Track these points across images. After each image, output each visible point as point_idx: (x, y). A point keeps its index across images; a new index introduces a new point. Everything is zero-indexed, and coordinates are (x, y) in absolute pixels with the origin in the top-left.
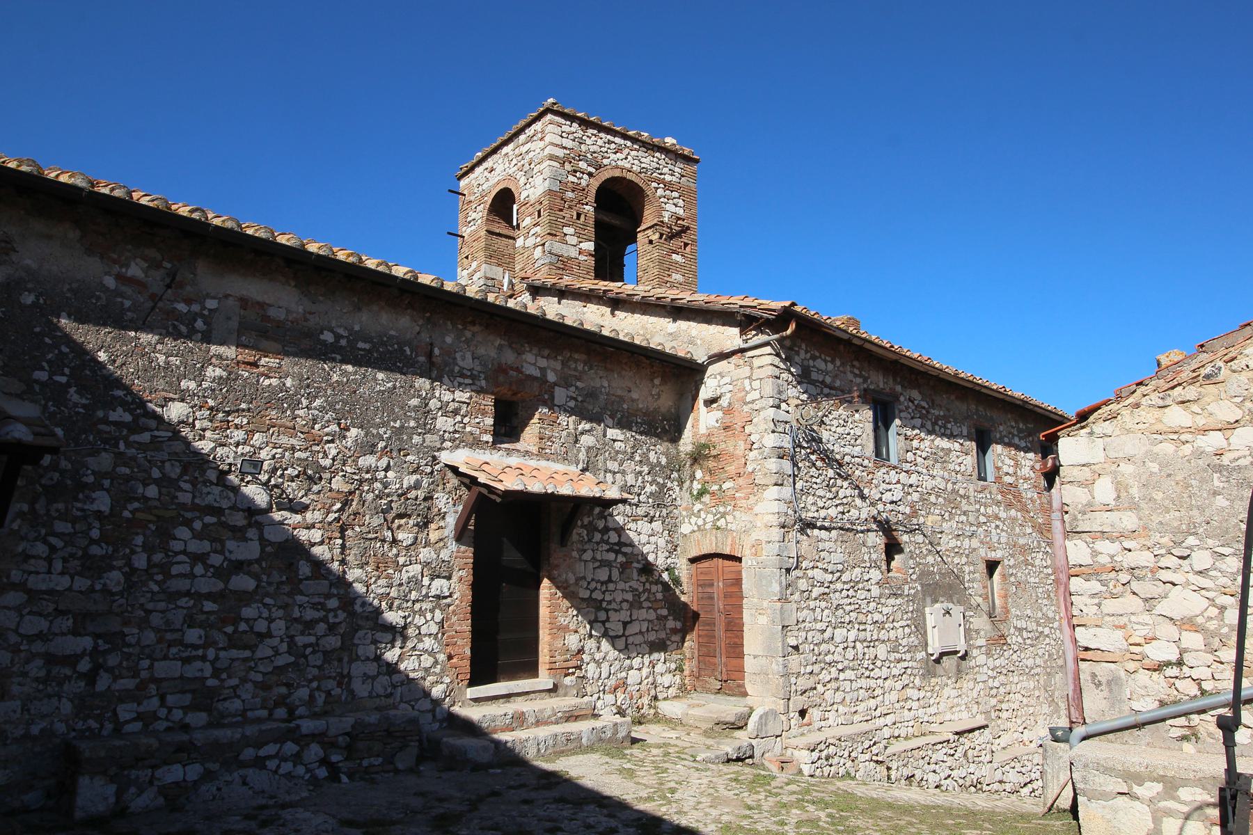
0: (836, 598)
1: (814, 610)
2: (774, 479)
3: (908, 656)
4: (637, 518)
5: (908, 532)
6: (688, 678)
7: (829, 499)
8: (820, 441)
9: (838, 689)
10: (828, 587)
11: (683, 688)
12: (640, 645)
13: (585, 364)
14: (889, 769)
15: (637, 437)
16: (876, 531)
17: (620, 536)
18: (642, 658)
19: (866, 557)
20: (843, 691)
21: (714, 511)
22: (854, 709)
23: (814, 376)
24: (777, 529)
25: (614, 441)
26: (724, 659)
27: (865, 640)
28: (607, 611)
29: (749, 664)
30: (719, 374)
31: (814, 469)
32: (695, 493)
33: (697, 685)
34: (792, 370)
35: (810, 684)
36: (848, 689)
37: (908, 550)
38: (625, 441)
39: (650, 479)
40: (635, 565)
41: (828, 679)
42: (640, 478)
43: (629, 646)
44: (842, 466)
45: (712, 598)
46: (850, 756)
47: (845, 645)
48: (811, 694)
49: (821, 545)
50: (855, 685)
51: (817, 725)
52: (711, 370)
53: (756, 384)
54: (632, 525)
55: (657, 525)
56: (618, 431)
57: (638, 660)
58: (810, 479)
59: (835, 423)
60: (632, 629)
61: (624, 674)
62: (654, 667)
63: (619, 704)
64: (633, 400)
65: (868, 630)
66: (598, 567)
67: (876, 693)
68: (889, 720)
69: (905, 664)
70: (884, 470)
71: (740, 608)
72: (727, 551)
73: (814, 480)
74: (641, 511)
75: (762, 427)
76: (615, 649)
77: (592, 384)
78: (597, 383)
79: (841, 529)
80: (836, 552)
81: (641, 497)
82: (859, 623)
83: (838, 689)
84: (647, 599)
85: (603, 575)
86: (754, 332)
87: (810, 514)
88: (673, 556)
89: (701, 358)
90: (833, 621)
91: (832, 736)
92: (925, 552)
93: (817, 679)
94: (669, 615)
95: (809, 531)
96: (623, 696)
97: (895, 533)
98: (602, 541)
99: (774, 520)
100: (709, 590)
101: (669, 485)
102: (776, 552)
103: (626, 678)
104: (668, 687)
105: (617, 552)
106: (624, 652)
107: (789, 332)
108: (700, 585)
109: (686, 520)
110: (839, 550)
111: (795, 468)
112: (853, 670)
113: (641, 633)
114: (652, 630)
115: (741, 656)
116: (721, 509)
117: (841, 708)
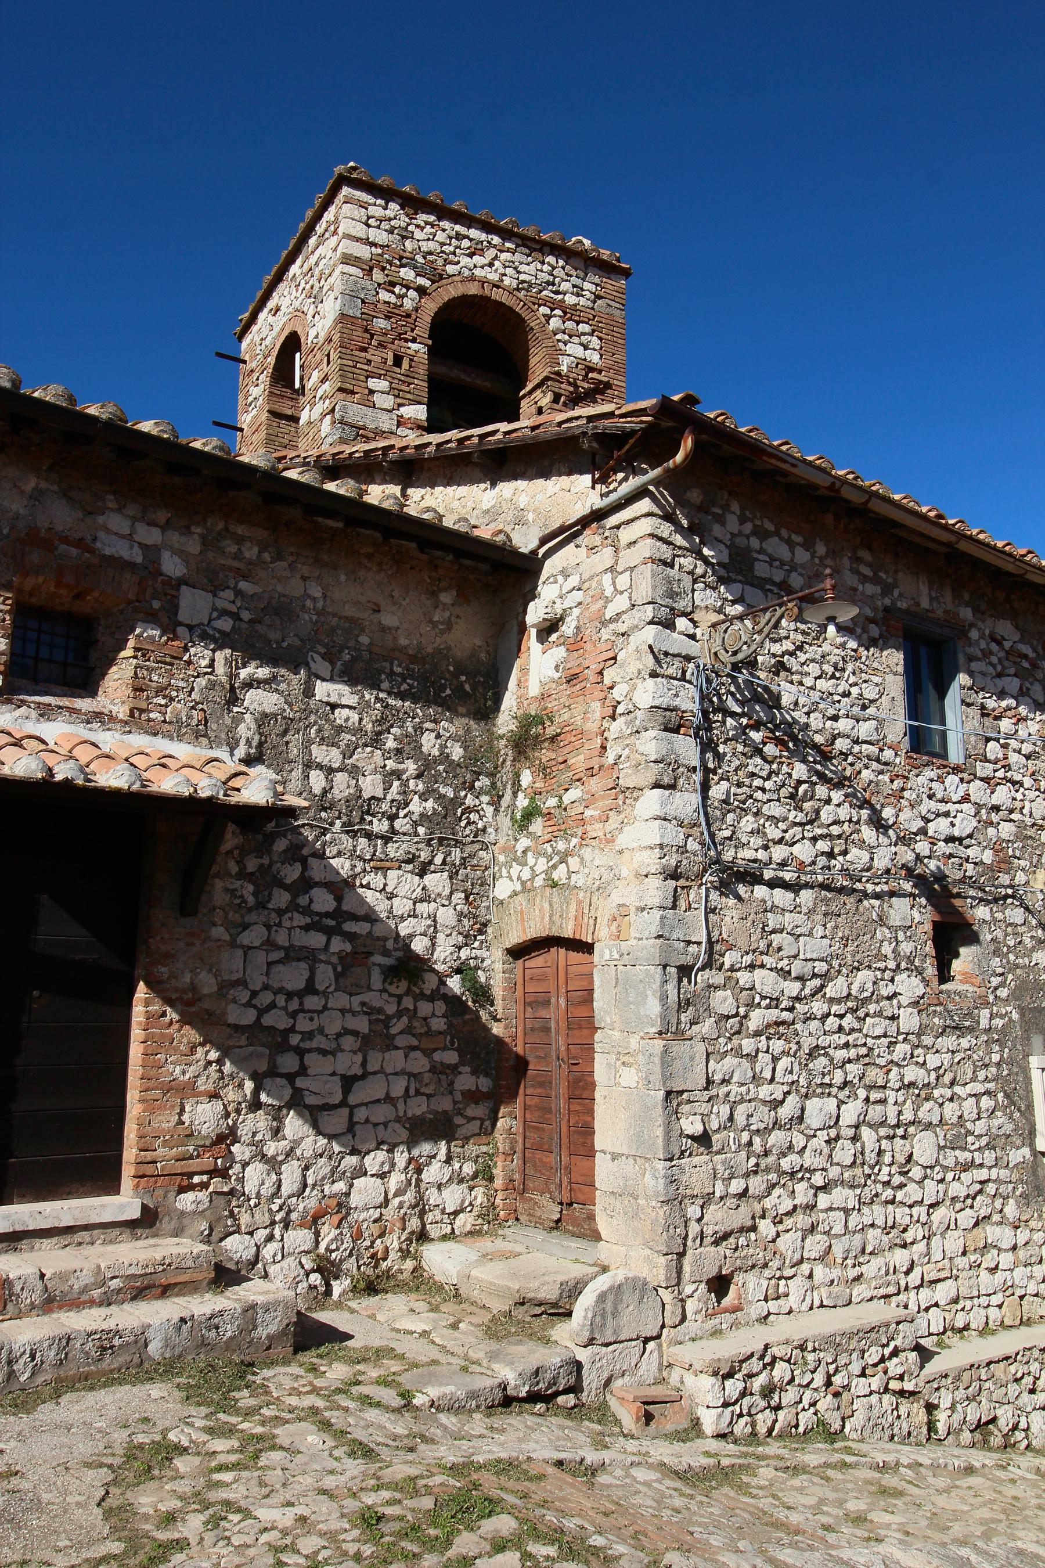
0: (809, 1034)
3: (989, 1157)
4: (388, 864)
6: (500, 1195)
7: (795, 824)
8: (774, 701)
9: (813, 1229)
10: (791, 1009)
11: (489, 1214)
12: (385, 1125)
14: (930, 1408)
15: (392, 702)
17: (339, 899)
18: (390, 1151)
19: (887, 949)
20: (827, 1233)
21: (550, 850)
22: (853, 1273)
23: (761, 569)
25: (334, 707)
26: (565, 1159)
27: (883, 1124)
28: (301, 1052)
29: (605, 1172)
31: (758, 760)
32: (518, 816)
33: (519, 1209)
34: (706, 551)
36: (838, 1229)
37: (989, 937)
38: (362, 707)
39: (421, 787)
40: (378, 959)
41: (787, 1205)
42: (396, 783)
43: (357, 1128)
44: (830, 759)
45: (547, 1030)
47: (833, 1133)
50: (854, 1220)
51: (757, 1309)
52: (549, 568)
53: (623, 581)
54: (376, 880)
55: (436, 882)
56: (345, 689)
57: (381, 1155)
58: (747, 781)
59: (813, 669)
60: (359, 1094)
61: (340, 1186)
62: (419, 1171)
64: (384, 629)
65: (891, 1101)
66: (279, 962)
67: (909, 1237)
68: (943, 1292)
69: (982, 1174)
70: (929, 773)
71: (588, 1049)
72: (568, 932)
73: (757, 782)
74: (394, 850)
75: (632, 669)
76: (319, 1133)
79: (824, 886)
80: (810, 935)
81: (398, 824)
82: (870, 1088)
83: (813, 1229)
84: (408, 1031)
85: (294, 977)
87: (748, 854)
88: (476, 944)
89: (525, 542)
90: (803, 1081)
92: (1028, 942)
94: (462, 1062)
95: (741, 889)
96: (334, 1232)
97: (957, 902)
99: (652, 861)
100: (543, 1013)
101: (470, 801)
103: (348, 1194)
104: (456, 1213)
105: (329, 932)
106: (343, 1139)
108: (530, 1004)
110: (819, 931)
112: (853, 1187)
113: (389, 1099)
114: (418, 1093)
115: (590, 1153)
116: (561, 846)
117: (821, 1272)
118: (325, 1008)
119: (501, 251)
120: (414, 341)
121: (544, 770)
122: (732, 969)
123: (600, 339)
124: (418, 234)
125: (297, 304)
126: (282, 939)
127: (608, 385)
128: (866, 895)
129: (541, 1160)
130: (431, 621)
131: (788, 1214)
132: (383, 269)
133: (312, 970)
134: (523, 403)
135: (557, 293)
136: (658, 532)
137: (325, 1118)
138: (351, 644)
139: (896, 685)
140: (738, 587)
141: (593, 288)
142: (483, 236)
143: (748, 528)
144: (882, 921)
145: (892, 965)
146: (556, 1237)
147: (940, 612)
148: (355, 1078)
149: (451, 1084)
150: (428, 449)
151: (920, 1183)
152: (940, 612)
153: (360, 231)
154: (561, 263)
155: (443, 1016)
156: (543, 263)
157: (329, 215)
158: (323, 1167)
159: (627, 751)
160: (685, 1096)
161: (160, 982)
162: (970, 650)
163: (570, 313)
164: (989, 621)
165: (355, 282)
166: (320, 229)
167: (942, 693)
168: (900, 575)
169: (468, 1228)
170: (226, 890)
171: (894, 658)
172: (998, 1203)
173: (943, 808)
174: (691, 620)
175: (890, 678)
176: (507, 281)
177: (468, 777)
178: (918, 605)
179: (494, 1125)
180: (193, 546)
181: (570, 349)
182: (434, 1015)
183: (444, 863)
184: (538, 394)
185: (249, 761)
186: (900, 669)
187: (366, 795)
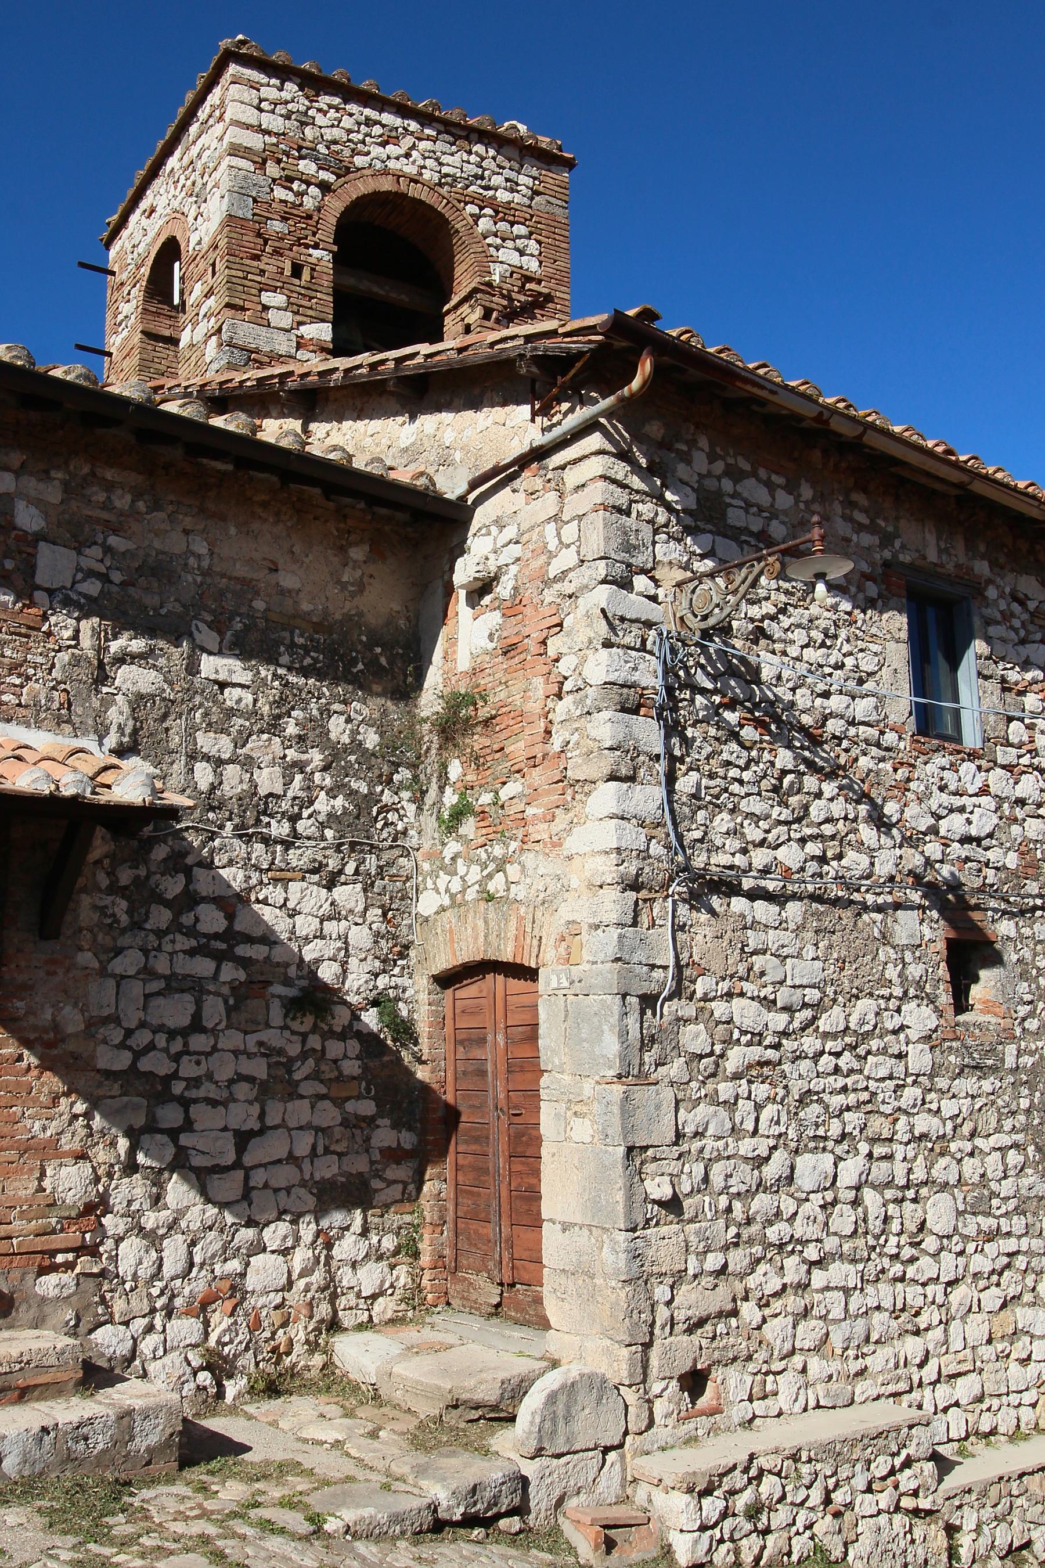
1: (731, 1105)
2: (606, 763)
3: (1018, 1224)
4: (289, 875)
5: (1013, 915)
6: (427, 1275)
7: (780, 823)
8: (752, 675)
9: (806, 1313)
10: (777, 1046)
11: (414, 1298)
12: (288, 1190)
13: (137, 496)
14: (951, 1530)
15: (292, 679)
16: (920, 907)
17: (230, 917)
18: (294, 1222)
19: (892, 973)
21: (484, 856)
22: (855, 1366)
23: (735, 517)
24: (612, 894)
25: (223, 685)
26: (506, 1231)
27: (889, 1184)
28: (186, 1103)
30: (496, 522)
31: (734, 746)
33: (451, 1292)
34: (669, 496)
35: (720, 1299)
36: (837, 1312)
38: (257, 686)
39: (328, 782)
40: (278, 989)
41: (774, 1284)
42: (298, 777)
43: (254, 1194)
44: (821, 744)
45: (483, 1073)
46: (827, 1501)
47: (829, 1196)
48: (721, 1328)
49: (754, 940)
51: (739, 1411)
52: (481, 516)
53: (570, 532)
54: (276, 894)
55: (348, 895)
56: (236, 664)
57: (283, 1227)
58: (721, 772)
59: (799, 636)
60: (256, 1153)
61: (234, 1265)
62: (329, 1246)
63: (212, 1342)
64: (283, 592)
65: (899, 1156)
66: (159, 993)
67: (922, 1321)
68: (965, 1389)
69: (1011, 1244)
70: (941, 760)
71: (534, 1096)
72: (507, 955)
73: (733, 773)
74: (296, 858)
75: (582, 637)
76: (208, 1200)
77: (157, 544)
78: (176, 543)
79: (814, 898)
80: (799, 956)
81: (300, 826)
82: (873, 1141)
83: (806, 1313)
84: (315, 1076)
86: (565, 406)
87: (723, 859)
88: (396, 971)
90: (792, 1134)
91: (771, 1446)
93: (739, 1287)
94: (380, 1114)
95: (716, 902)
96: (228, 1321)
98: (177, 926)
99: (607, 869)
100: (478, 1053)
101: (387, 798)
102: (612, 950)
103: (243, 1275)
104: (374, 1297)
105: (220, 958)
106: (237, 1207)
107: (636, 384)
108: (462, 1042)
109: (430, 884)
110: (810, 952)
111: (675, 741)
112: (854, 1261)
113: (292, 1159)
114: (327, 1151)
115: (537, 1223)
116: (498, 851)
117: (816, 1366)
118: (215, 1049)
119: (420, 139)
120: (316, 246)
121: (477, 761)
122: (705, 999)
123: (539, 243)
124: (320, 120)
125: (175, 204)
126: (162, 966)
127: (549, 298)
128: (865, 908)
129: (476, 1232)
130: (339, 582)
131: (776, 1295)
132: (279, 161)
133: (199, 1004)
134: (448, 320)
135: (487, 188)
136: (611, 473)
137: (215, 1183)
138: (244, 610)
139: (899, 655)
140: (708, 537)
141: (530, 182)
142: (398, 122)
143: (719, 467)
144: (885, 938)
145: (898, 992)
146: (495, 1320)
147: (950, 567)
148: (251, 1134)
149: (367, 1140)
150: (334, 376)
151: (936, 1256)
152: (950, 567)
153: (250, 116)
154: (492, 152)
155: (357, 1058)
156: (470, 153)
157: (214, 98)
158: (213, 1242)
159: (575, 737)
160: (650, 1152)
161: (15, 1020)
162: (988, 612)
163: (502, 212)
164: (1010, 577)
165: (245, 178)
166: (202, 114)
167: (954, 664)
168: (903, 523)
169: (389, 1315)
170: (95, 907)
171: (897, 622)
172: (1030, 1280)
173: (957, 801)
174: (652, 579)
175: (891, 646)
176: (427, 175)
177: (386, 769)
178: (924, 558)
179: (419, 1189)
180: (53, 494)
181: (502, 255)
182: (345, 1056)
183: (357, 872)
184: (465, 309)
185: (121, 752)
186: (904, 635)
187: (262, 792)
